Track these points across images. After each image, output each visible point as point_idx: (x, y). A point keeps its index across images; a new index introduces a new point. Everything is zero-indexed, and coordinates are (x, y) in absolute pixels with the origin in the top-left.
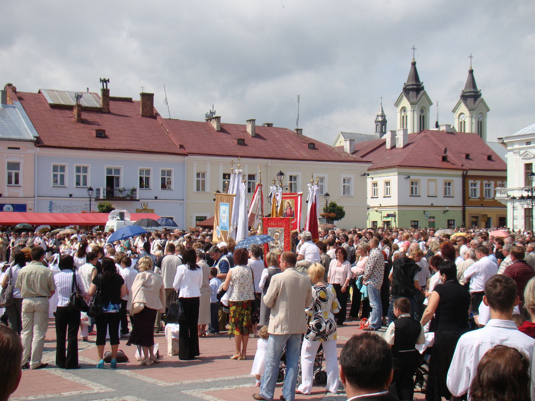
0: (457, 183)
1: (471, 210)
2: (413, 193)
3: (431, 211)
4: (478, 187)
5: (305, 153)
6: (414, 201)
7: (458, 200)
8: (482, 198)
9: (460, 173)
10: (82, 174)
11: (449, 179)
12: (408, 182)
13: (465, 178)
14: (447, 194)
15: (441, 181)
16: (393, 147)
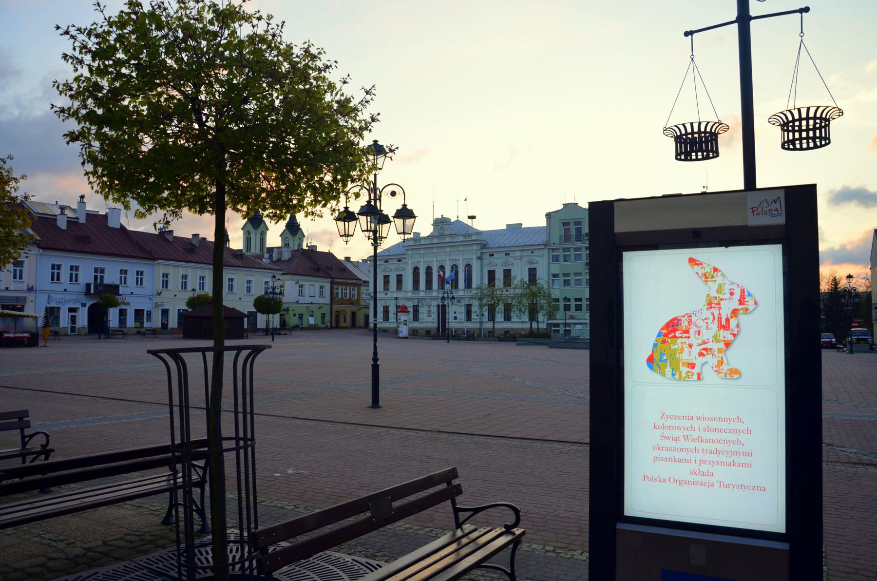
0: (327, 286)
1: (336, 307)
2: (301, 294)
3: (312, 308)
4: (340, 291)
5: (236, 262)
6: (302, 300)
7: (327, 300)
8: (342, 298)
9: (329, 280)
10: (56, 271)
11: (322, 284)
12: (297, 286)
13: (332, 284)
14: (321, 294)
15: (318, 285)
16: (279, 260)
